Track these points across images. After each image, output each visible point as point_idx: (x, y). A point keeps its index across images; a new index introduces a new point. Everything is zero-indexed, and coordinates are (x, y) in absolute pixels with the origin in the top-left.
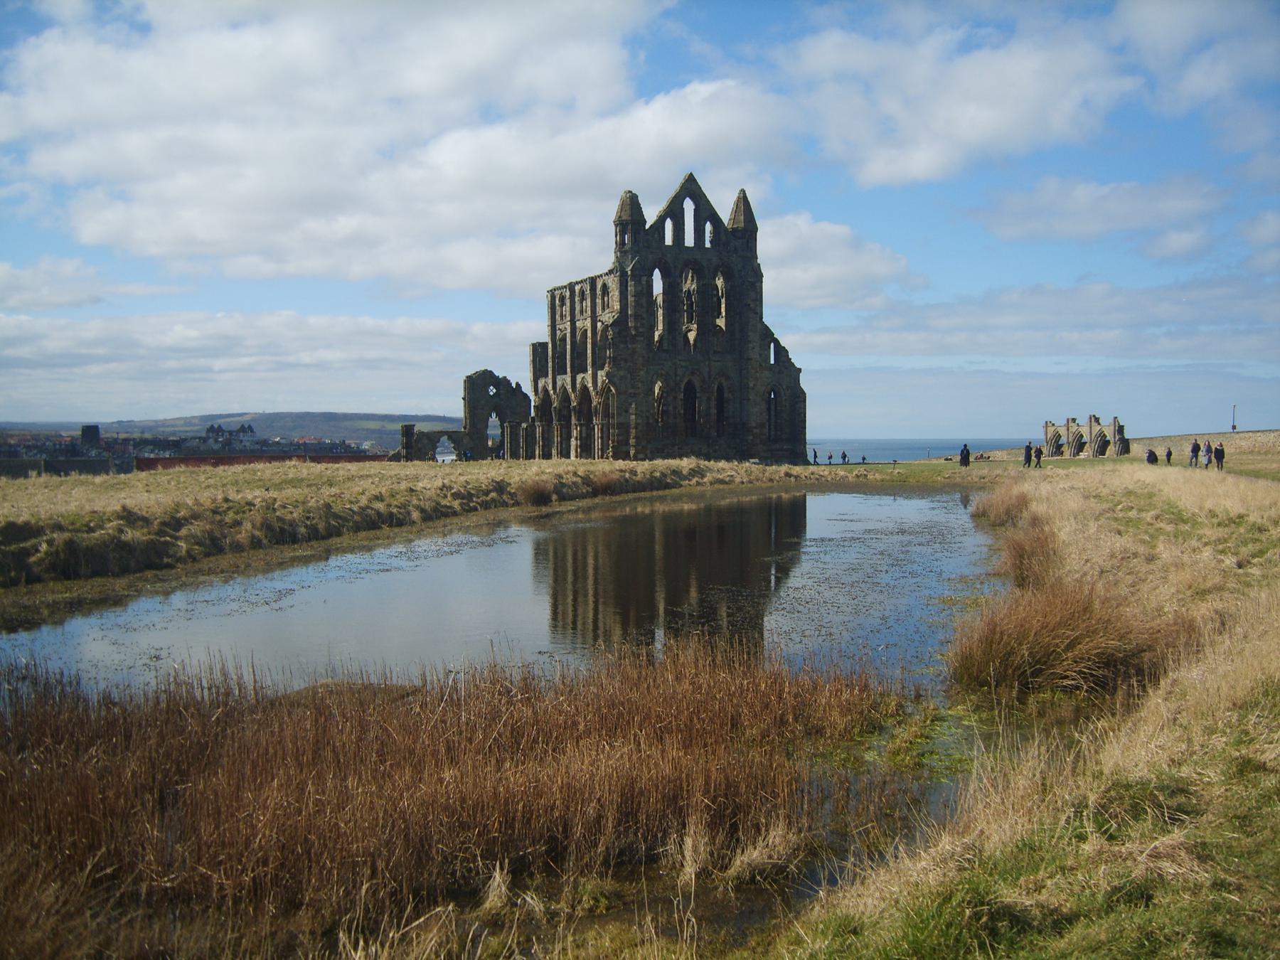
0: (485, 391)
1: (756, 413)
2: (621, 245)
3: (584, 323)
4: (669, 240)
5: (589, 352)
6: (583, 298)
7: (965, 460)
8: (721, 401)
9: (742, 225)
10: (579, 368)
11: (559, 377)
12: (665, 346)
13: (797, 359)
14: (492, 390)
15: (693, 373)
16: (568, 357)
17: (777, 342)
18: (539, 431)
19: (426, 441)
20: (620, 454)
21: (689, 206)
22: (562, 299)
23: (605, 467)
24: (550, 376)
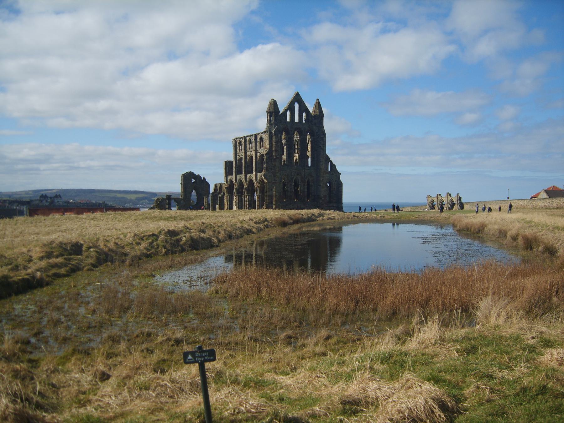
1: (323, 192)
2: (269, 121)
4: (288, 120)
5: (254, 165)
9: (318, 114)
10: (249, 170)
11: (238, 176)
13: (339, 169)
15: (298, 174)
16: (243, 167)
17: (331, 162)
21: (297, 106)
23: (273, 214)
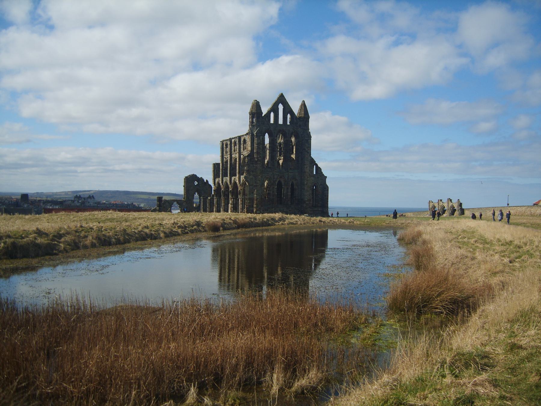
0: (193, 183)
1: (307, 195)
2: (252, 123)
3: (236, 155)
4: (272, 121)
5: (237, 167)
6: (235, 145)
7: (395, 215)
8: (293, 189)
9: (303, 115)
10: (233, 174)
12: (270, 166)
14: (196, 183)
15: (281, 177)
16: (228, 170)
17: (317, 165)
18: (215, 200)
19: (167, 204)
20: (250, 211)
21: (281, 107)
22: (227, 145)
23: (243, 216)
24: (221, 177)
